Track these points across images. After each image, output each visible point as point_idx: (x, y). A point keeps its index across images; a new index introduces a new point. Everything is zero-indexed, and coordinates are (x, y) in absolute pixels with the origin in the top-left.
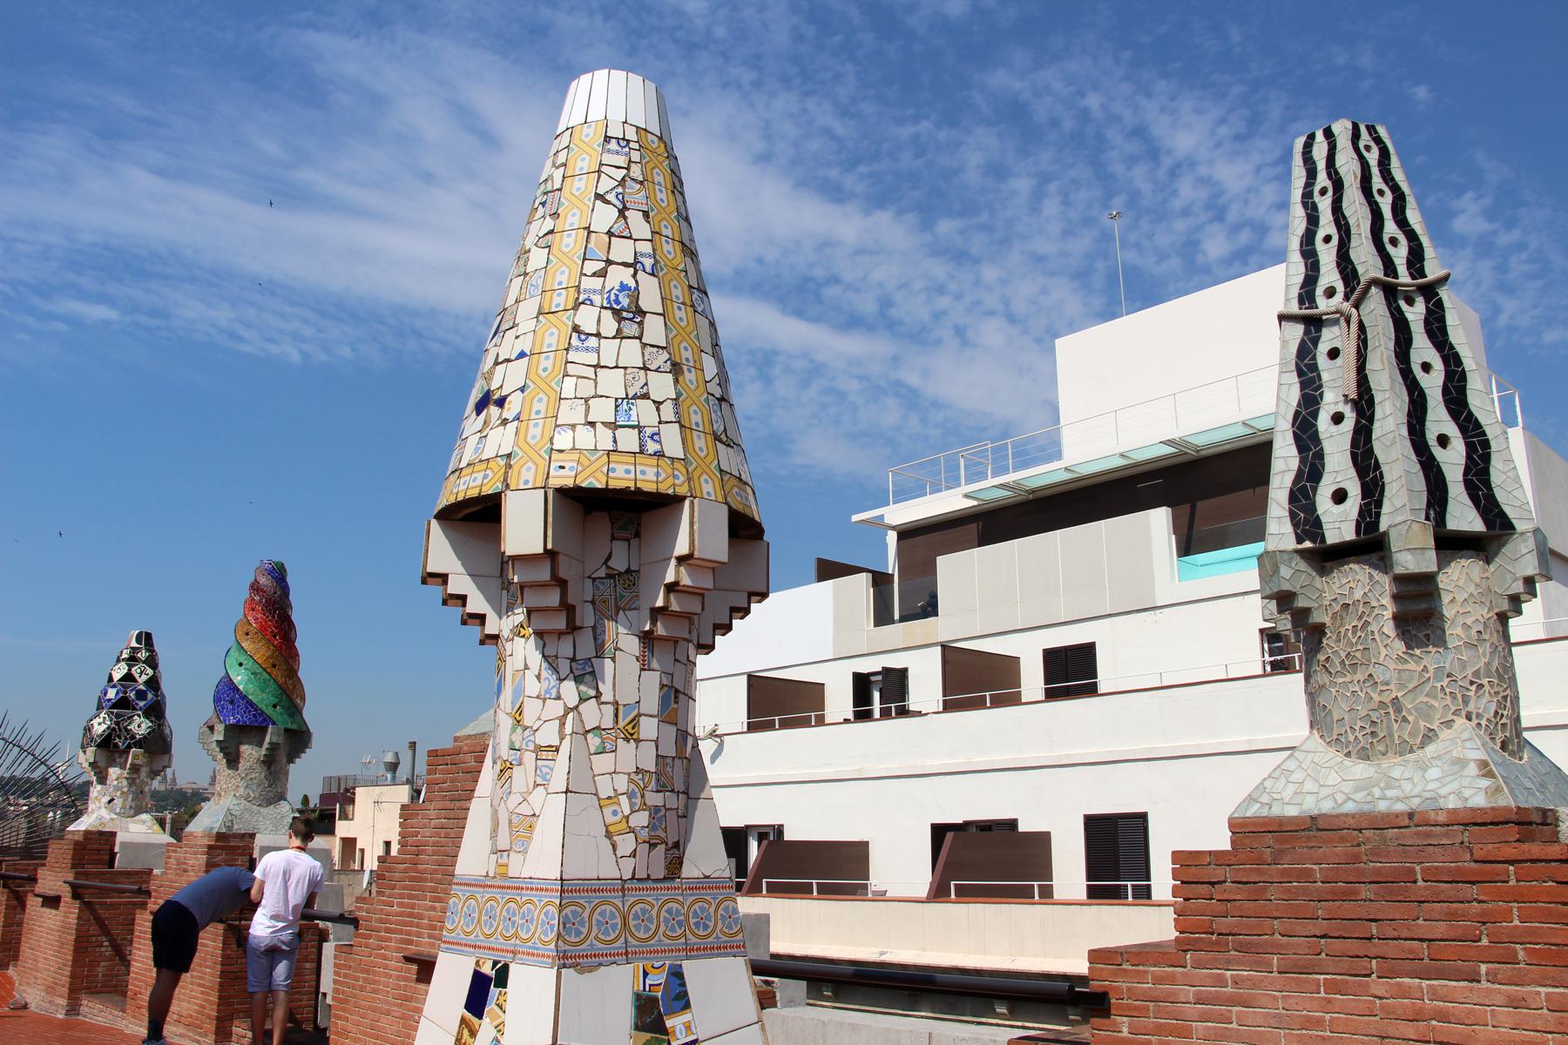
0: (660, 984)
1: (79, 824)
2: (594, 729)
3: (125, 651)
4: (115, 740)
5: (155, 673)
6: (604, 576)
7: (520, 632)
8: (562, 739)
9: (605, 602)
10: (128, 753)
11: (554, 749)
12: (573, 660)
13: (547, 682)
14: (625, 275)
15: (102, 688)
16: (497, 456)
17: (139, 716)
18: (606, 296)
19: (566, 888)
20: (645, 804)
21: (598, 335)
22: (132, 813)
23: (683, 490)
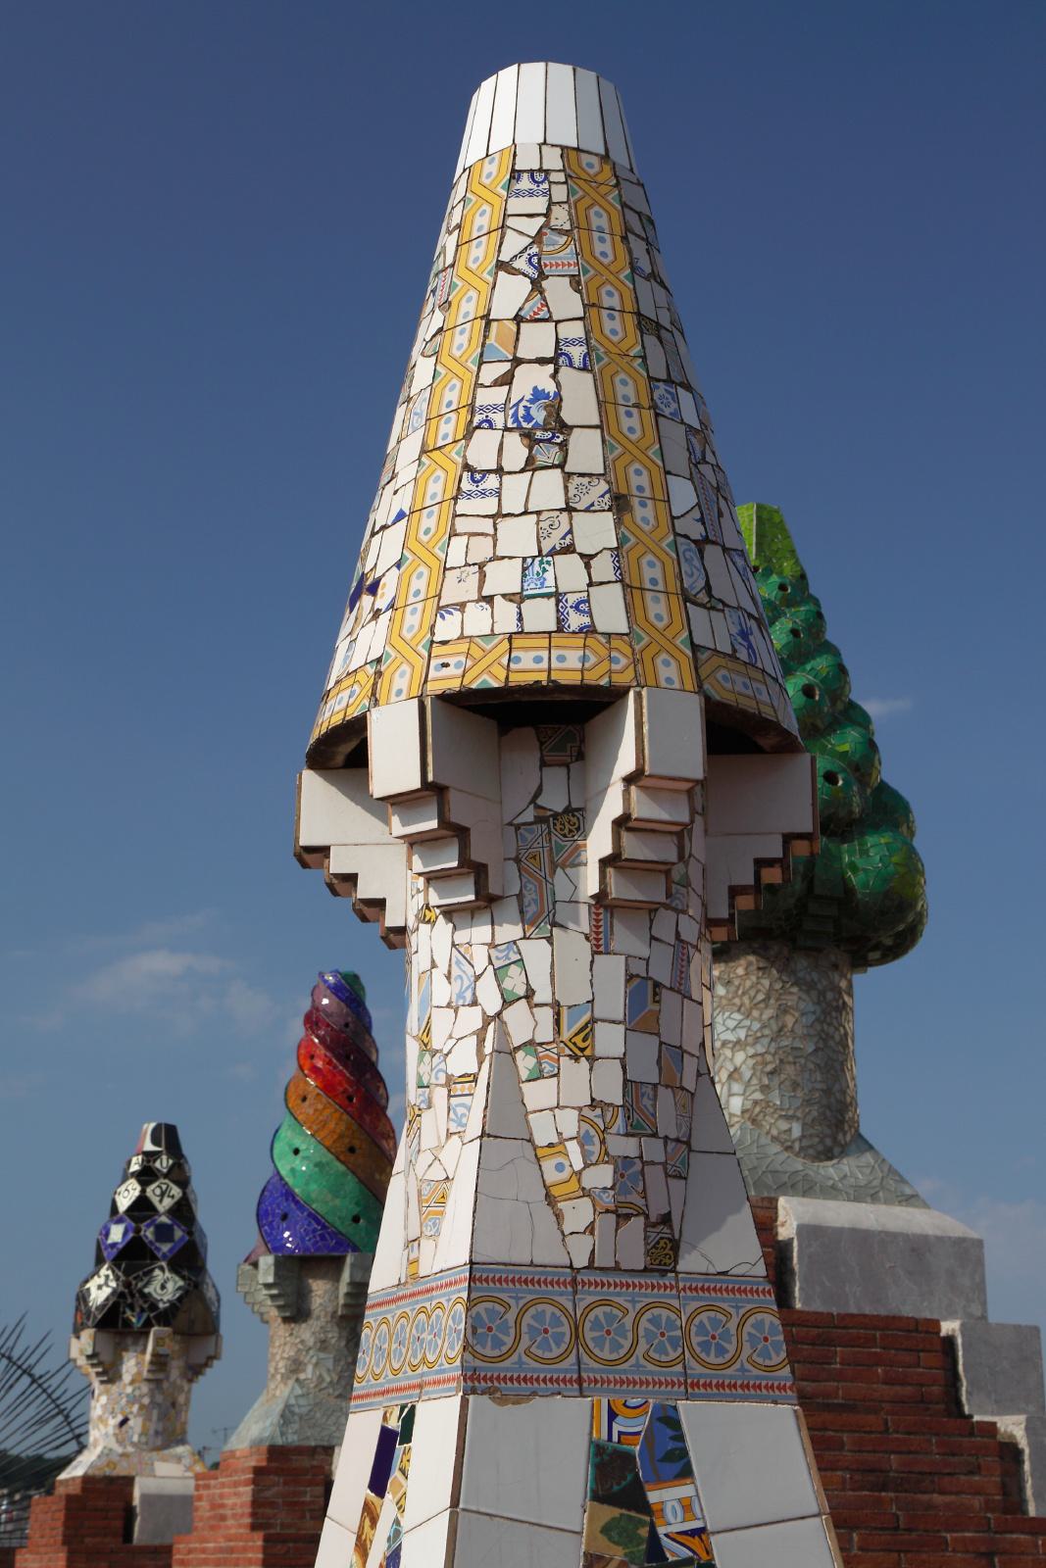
0: (638, 1433)
2: (525, 1044)
3: (134, 1160)
4: (124, 1312)
5: (184, 1194)
6: (532, 819)
7: (425, 916)
8: (480, 1063)
9: (534, 857)
10: (147, 1334)
11: (471, 1078)
12: (492, 945)
13: (459, 981)
14: (540, 378)
15: (102, 1224)
16: (366, 664)
17: (162, 1269)
18: (511, 412)
19: (478, 1275)
20: (607, 1153)
21: (499, 471)
22: (159, 1442)
23: (623, 679)
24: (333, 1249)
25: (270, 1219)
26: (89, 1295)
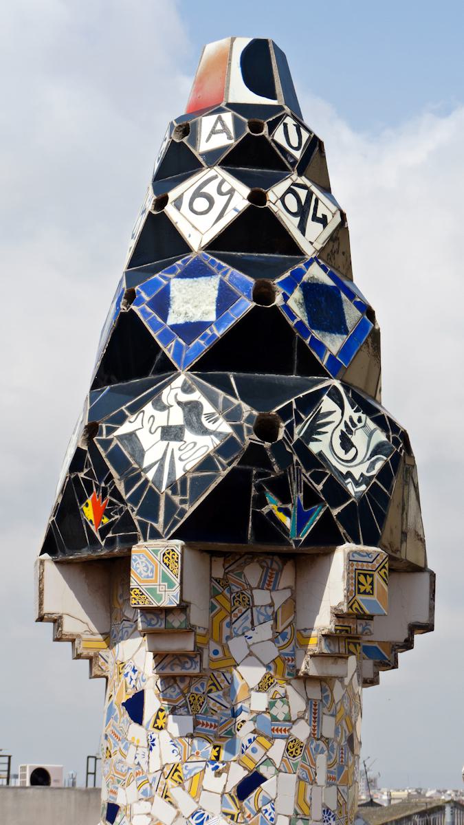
26: (140, 453)
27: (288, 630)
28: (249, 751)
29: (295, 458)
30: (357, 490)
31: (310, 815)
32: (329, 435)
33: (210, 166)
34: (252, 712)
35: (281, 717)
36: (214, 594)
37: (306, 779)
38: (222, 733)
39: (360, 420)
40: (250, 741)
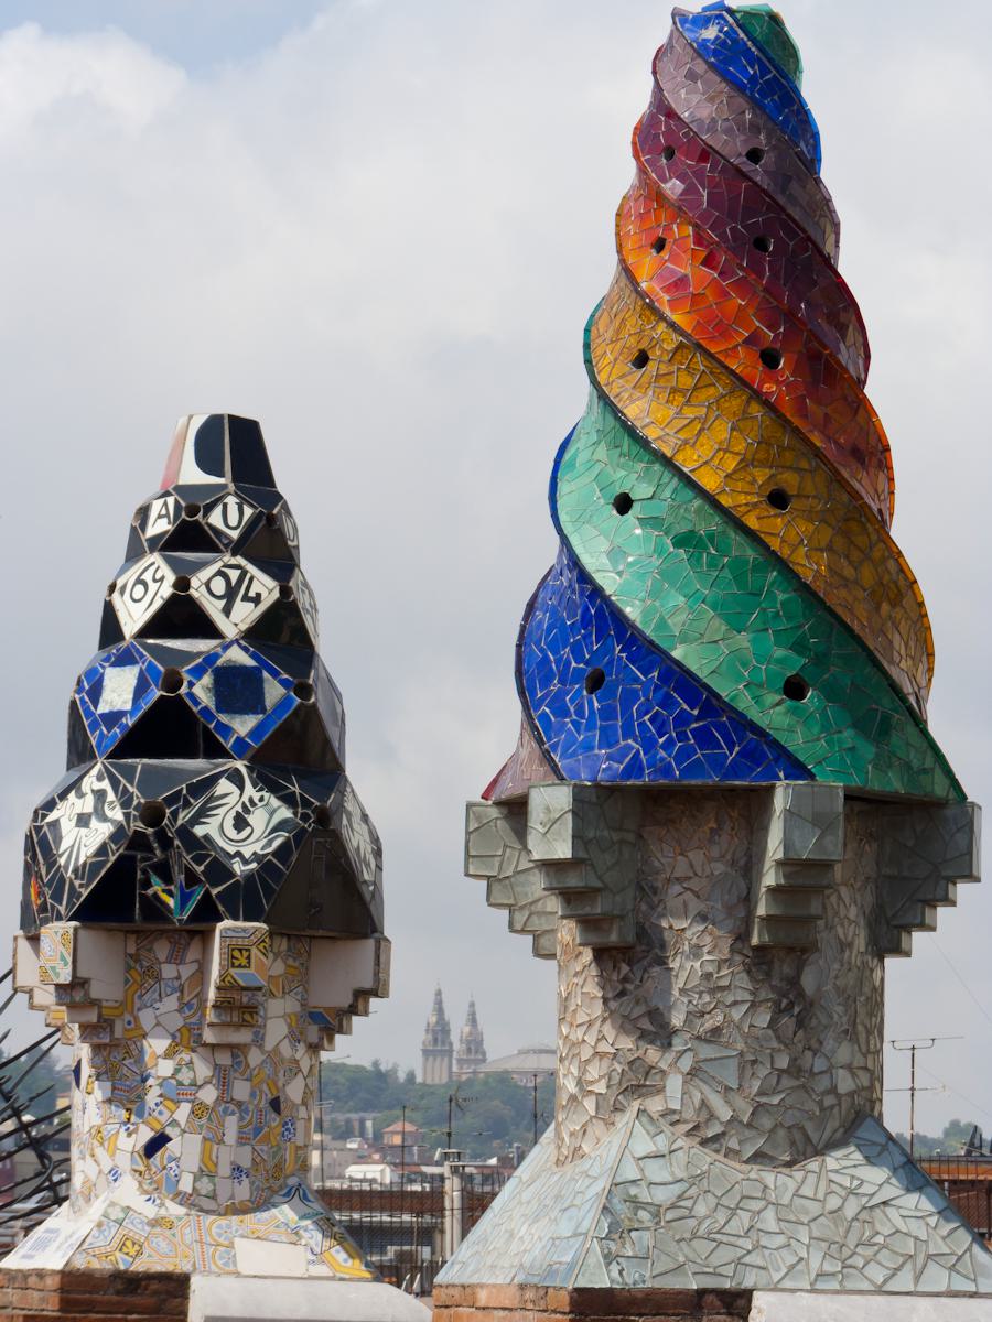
1: (42, 1245)
4: (147, 884)
5: (285, 591)
10: (206, 937)
15: (80, 668)
24: (734, 770)
25: (555, 686)
27: (195, 1001)
28: (156, 1114)
29: (177, 842)
30: (243, 868)
31: (216, 1172)
32: (220, 818)
33: (152, 551)
34: (158, 1077)
35: (186, 1082)
36: (128, 969)
37: (214, 1139)
38: (132, 1097)
39: (261, 799)
40: (157, 1104)
